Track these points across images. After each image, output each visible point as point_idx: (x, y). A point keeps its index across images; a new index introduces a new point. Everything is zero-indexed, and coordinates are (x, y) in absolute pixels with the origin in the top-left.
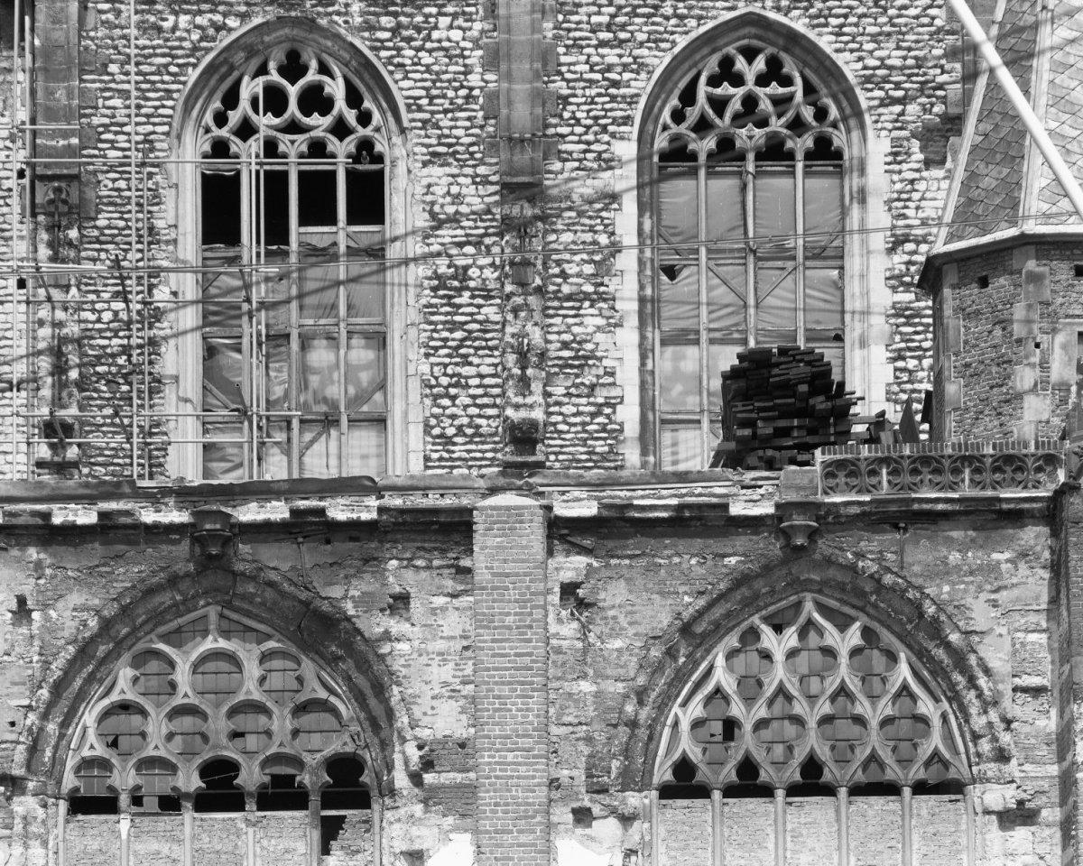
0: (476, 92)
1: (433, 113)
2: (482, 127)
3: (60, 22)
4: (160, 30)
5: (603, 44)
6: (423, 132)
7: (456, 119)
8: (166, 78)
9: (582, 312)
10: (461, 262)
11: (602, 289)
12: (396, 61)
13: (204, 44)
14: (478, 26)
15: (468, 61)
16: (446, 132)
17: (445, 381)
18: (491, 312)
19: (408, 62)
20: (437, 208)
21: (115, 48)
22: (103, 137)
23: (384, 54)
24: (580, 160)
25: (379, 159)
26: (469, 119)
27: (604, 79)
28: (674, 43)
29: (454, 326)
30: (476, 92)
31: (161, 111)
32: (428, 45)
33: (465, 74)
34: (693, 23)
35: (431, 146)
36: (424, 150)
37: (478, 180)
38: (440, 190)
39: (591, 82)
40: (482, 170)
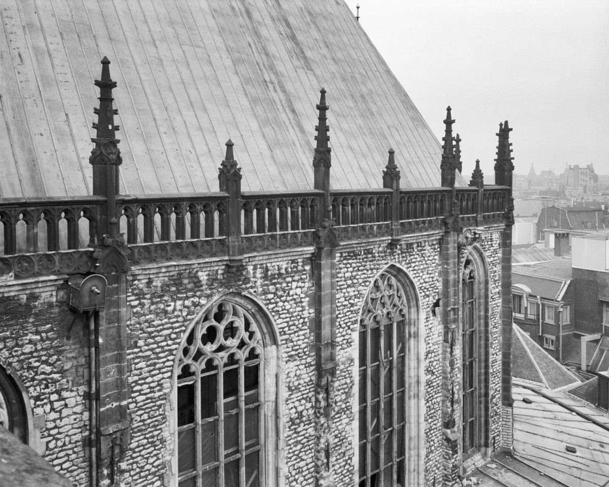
0: (306, 320)
1: (290, 334)
2: (308, 338)
3: (113, 322)
4: (166, 312)
5: (349, 286)
6: (286, 346)
7: (298, 336)
8: (170, 342)
9: (341, 418)
10: (300, 409)
11: (348, 404)
12: (275, 310)
13: (189, 317)
14: (307, 285)
15: (303, 304)
16: (295, 343)
17: (294, 473)
18: (311, 431)
19: (280, 309)
20: (291, 385)
21: (142, 329)
22: (135, 389)
23: (271, 306)
24: (341, 345)
25: (257, 356)
26: (304, 335)
27: (350, 303)
28: (370, 282)
29: (298, 442)
30: (306, 320)
31: (167, 364)
32: (289, 298)
33: (302, 311)
34: (375, 271)
35: (289, 352)
36: (286, 355)
37: (307, 365)
38: (292, 375)
39: (345, 306)
40: (309, 360)
